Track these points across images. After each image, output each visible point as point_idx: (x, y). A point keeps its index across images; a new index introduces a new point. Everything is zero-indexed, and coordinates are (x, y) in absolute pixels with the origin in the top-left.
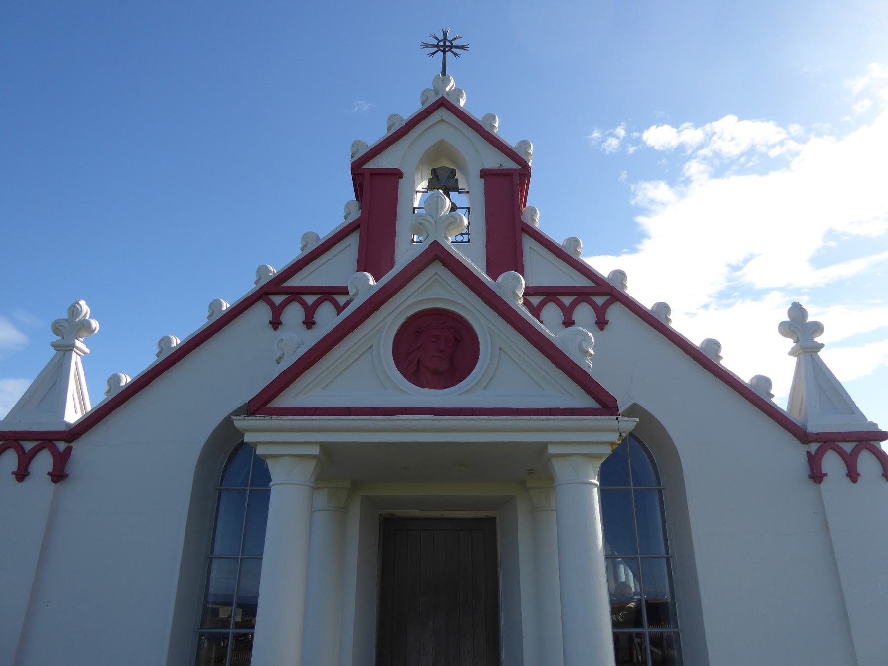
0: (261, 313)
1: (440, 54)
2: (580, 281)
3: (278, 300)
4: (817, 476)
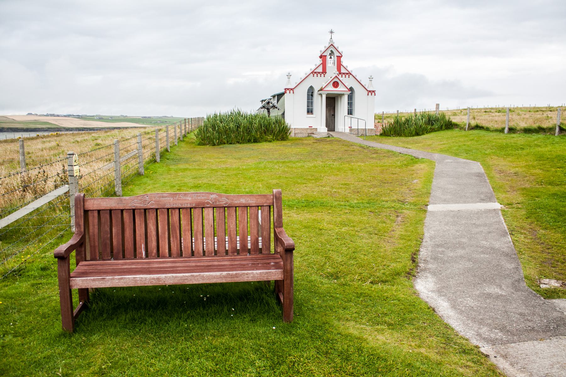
0: (312, 74)
2: (348, 72)
3: (314, 73)
4: (368, 95)
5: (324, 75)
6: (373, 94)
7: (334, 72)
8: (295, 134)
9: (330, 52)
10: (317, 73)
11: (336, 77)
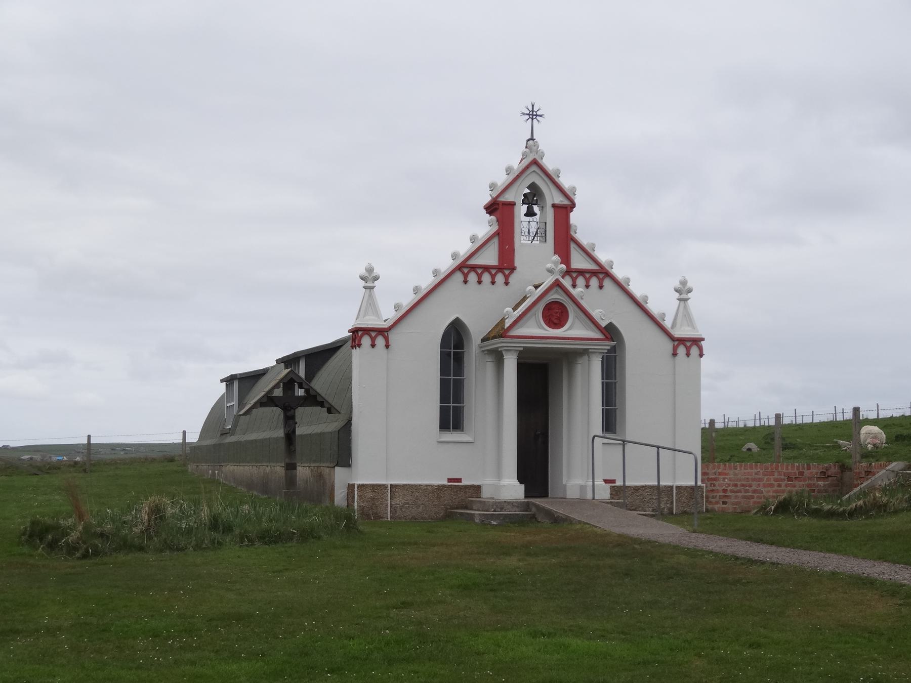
1: (530, 120)
2: (592, 266)
3: (466, 270)
4: (675, 354)
5: (507, 278)
6: (694, 350)
7: (549, 265)
8: (394, 509)
9: (527, 191)
10: (479, 271)
11: (557, 284)
